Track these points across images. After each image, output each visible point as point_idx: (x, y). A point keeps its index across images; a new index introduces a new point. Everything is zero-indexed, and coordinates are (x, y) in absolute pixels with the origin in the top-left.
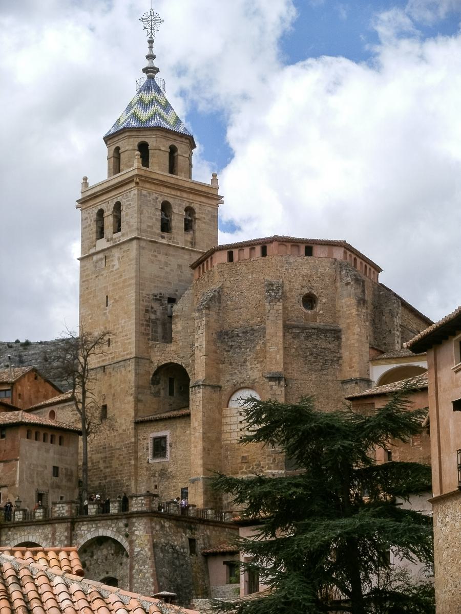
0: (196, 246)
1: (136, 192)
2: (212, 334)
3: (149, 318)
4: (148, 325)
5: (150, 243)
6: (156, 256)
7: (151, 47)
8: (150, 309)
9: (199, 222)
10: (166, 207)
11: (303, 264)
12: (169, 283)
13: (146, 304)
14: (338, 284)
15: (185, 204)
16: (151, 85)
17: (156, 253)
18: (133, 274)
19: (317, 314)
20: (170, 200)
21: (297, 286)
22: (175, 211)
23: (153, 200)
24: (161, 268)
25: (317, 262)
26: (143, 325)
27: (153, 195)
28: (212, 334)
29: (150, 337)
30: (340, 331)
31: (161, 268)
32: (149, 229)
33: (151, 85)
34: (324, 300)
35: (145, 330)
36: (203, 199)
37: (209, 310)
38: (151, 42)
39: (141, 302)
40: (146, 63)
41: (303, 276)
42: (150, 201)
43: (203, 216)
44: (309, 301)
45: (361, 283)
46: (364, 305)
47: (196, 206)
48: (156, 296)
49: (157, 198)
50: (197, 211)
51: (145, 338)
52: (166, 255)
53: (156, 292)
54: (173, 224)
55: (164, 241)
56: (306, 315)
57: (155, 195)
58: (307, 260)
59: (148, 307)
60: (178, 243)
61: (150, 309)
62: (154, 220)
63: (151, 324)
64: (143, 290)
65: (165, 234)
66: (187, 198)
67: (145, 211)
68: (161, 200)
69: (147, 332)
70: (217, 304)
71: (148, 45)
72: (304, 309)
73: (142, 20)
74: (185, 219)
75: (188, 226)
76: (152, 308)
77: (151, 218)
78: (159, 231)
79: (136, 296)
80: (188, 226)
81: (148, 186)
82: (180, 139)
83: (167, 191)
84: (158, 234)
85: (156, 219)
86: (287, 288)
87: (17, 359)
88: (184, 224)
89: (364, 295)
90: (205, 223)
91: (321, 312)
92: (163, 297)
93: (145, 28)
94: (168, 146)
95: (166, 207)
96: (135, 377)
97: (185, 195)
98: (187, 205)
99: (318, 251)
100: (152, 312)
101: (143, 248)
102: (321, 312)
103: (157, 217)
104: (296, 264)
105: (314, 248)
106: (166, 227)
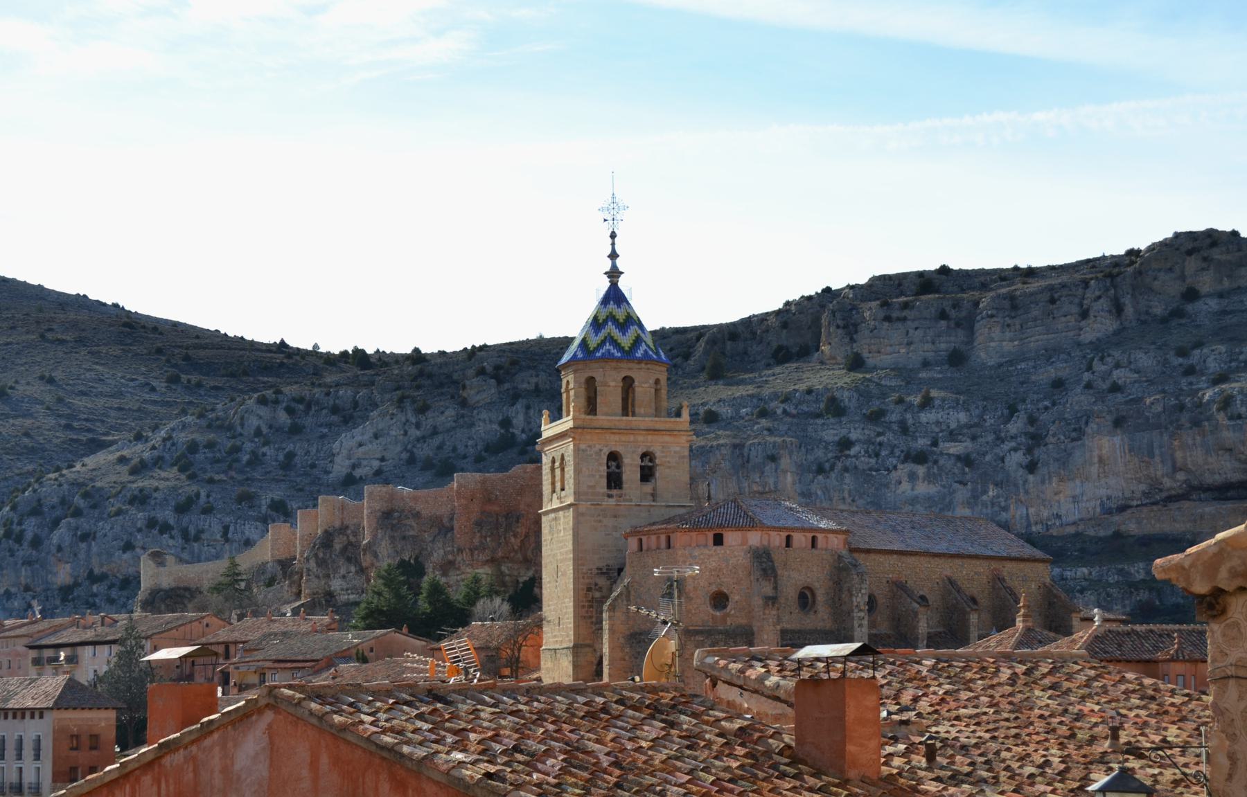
0: (658, 499)
1: (571, 447)
2: (618, 639)
3: (593, 598)
4: (591, 606)
5: (593, 507)
6: (600, 521)
7: (613, 244)
8: (593, 587)
9: (662, 467)
10: (613, 457)
11: (711, 556)
12: (620, 550)
13: (587, 581)
14: (752, 578)
15: (640, 451)
16: (614, 296)
17: (599, 518)
18: (570, 547)
19: (728, 615)
20: (620, 449)
22: (626, 461)
23: (596, 453)
24: (609, 535)
25: (728, 552)
26: (583, 606)
27: (595, 447)
28: (618, 639)
29: (594, 620)
30: (753, 634)
31: (609, 535)
32: (590, 491)
33: (614, 296)
34: (737, 598)
35: (587, 612)
36: (667, 438)
37: (614, 612)
38: (613, 236)
39: (582, 580)
40: (607, 265)
41: (710, 571)
42: (591, 455)
43: (668, 459)
44: (719, 600)
45: (772, 579)
46: (773, 606)
48: (601, 569)
49: (601, 450)
50: (658, 454)
51: (586, 623)
52: (615, 517)
53: (600, 565)
54: (624, 477)
56: (713, 617)
57: (598, 447)
58: (715, 551)
59: (590, 584)
60: (631, 501)
61: (593, 587)
62: (598, 477)
63: (595, 604)
64: (583, 565)
65: (614, 492)
66: (643, 442)
67: (584, 469)
68: (606, 451)
69: (590, 614)
70: (625, 602)
71: (610, 241)
72: (711, 611)
73: (600, 210)
74: (642, 468)
75: (647, 474)
76: (596, 585)
77: (593, 476)
78: (605, 490)
79: (574, 573)
80: (647, 474)
82: (637, 366)
83: (617, 437)
84: (603, 495)
85: (601, 476)
87: (1007, 304)
88: (639, 475)
89: (776, 593)
90: (669, 467)
91: (733, 612)
92: (611, 570)
93: (605, 220)
94: (620, 379)
95: (613, 457)
96: (574, 670)
97: (640, 438)
98: (645, 450)
100: (597, 590)
101: (582, 514)
102: (733, 612)
103: (602, 473)
104: (702, 557)
105: (724, 536)
106: (614, 481)
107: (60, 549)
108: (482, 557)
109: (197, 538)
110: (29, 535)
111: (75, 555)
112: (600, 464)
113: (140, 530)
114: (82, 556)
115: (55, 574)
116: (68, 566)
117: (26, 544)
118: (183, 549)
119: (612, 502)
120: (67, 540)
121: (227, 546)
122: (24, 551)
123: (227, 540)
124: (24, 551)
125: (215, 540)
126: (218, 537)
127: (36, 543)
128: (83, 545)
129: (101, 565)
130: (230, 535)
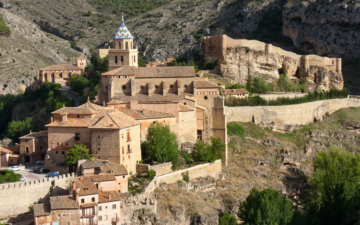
10: (116, 57)
15: (120, 56)
20: (117, 56)
21: (105, 84)
36: (125, 53)
47: (123, 56)
55: (116, 65)
65: (116, 63)
68: (114, 56)
75: (122, 60)
81: (111, 53)
86: (103, 85)
95: (116, 57)
97: (120, 54)
99: (108, 77)
101: (111, 68)
106: (116, 62)
107: (322, 14)
108: (210, 55)
109: (351, 12)
110: (318, 10)
111: (325, 16)
112: (114, 58)
113: (338, 9)
114: (326, 16)
115: (321, 21)
116: (324, 19)
117: (317, 12)
118: (347, 15)
119: (116, 65)
120: (324, 12)
121: (357, 14)
122: (316, 14)
123: (357, 12)
124: (316, 14)
125: (355, 12)
126: (355, 11)
127: (319, 12)
128: (327, 13)
129: (330, 19)
130: (358, 11)
